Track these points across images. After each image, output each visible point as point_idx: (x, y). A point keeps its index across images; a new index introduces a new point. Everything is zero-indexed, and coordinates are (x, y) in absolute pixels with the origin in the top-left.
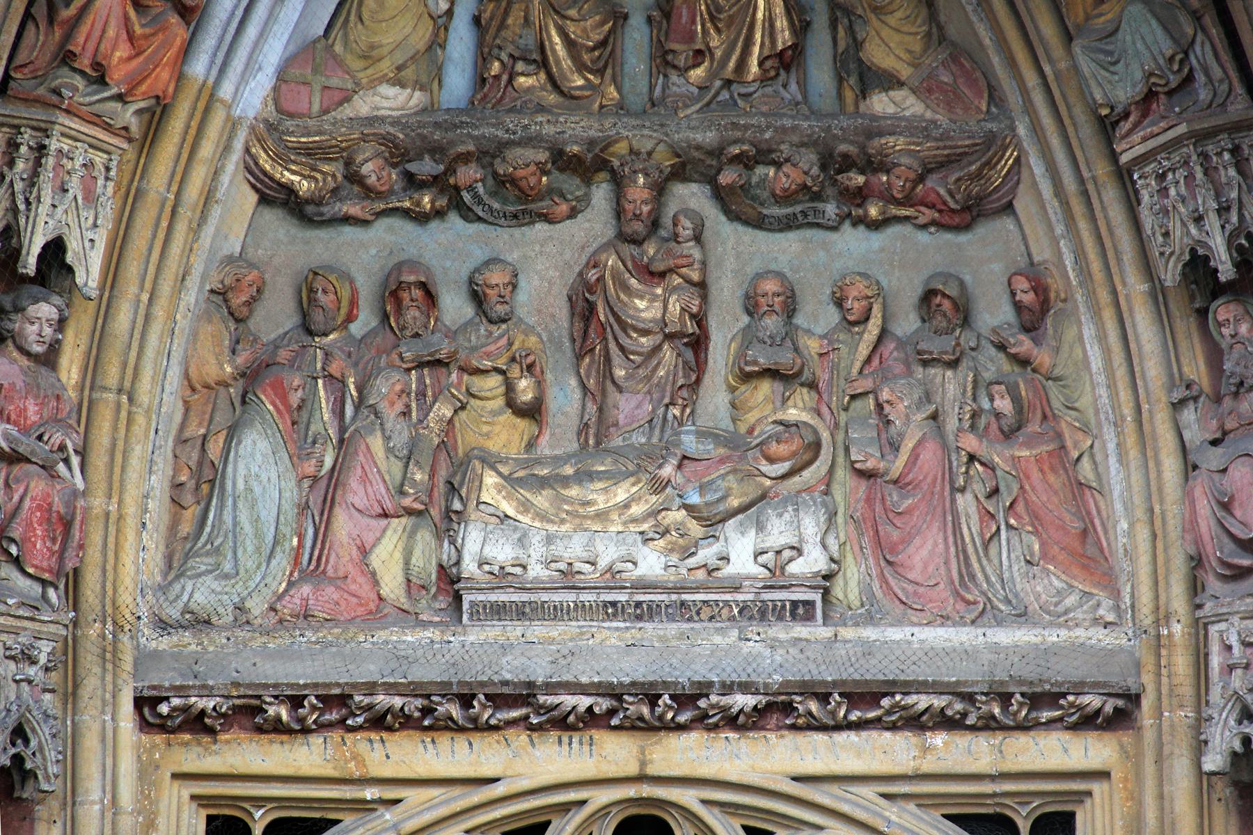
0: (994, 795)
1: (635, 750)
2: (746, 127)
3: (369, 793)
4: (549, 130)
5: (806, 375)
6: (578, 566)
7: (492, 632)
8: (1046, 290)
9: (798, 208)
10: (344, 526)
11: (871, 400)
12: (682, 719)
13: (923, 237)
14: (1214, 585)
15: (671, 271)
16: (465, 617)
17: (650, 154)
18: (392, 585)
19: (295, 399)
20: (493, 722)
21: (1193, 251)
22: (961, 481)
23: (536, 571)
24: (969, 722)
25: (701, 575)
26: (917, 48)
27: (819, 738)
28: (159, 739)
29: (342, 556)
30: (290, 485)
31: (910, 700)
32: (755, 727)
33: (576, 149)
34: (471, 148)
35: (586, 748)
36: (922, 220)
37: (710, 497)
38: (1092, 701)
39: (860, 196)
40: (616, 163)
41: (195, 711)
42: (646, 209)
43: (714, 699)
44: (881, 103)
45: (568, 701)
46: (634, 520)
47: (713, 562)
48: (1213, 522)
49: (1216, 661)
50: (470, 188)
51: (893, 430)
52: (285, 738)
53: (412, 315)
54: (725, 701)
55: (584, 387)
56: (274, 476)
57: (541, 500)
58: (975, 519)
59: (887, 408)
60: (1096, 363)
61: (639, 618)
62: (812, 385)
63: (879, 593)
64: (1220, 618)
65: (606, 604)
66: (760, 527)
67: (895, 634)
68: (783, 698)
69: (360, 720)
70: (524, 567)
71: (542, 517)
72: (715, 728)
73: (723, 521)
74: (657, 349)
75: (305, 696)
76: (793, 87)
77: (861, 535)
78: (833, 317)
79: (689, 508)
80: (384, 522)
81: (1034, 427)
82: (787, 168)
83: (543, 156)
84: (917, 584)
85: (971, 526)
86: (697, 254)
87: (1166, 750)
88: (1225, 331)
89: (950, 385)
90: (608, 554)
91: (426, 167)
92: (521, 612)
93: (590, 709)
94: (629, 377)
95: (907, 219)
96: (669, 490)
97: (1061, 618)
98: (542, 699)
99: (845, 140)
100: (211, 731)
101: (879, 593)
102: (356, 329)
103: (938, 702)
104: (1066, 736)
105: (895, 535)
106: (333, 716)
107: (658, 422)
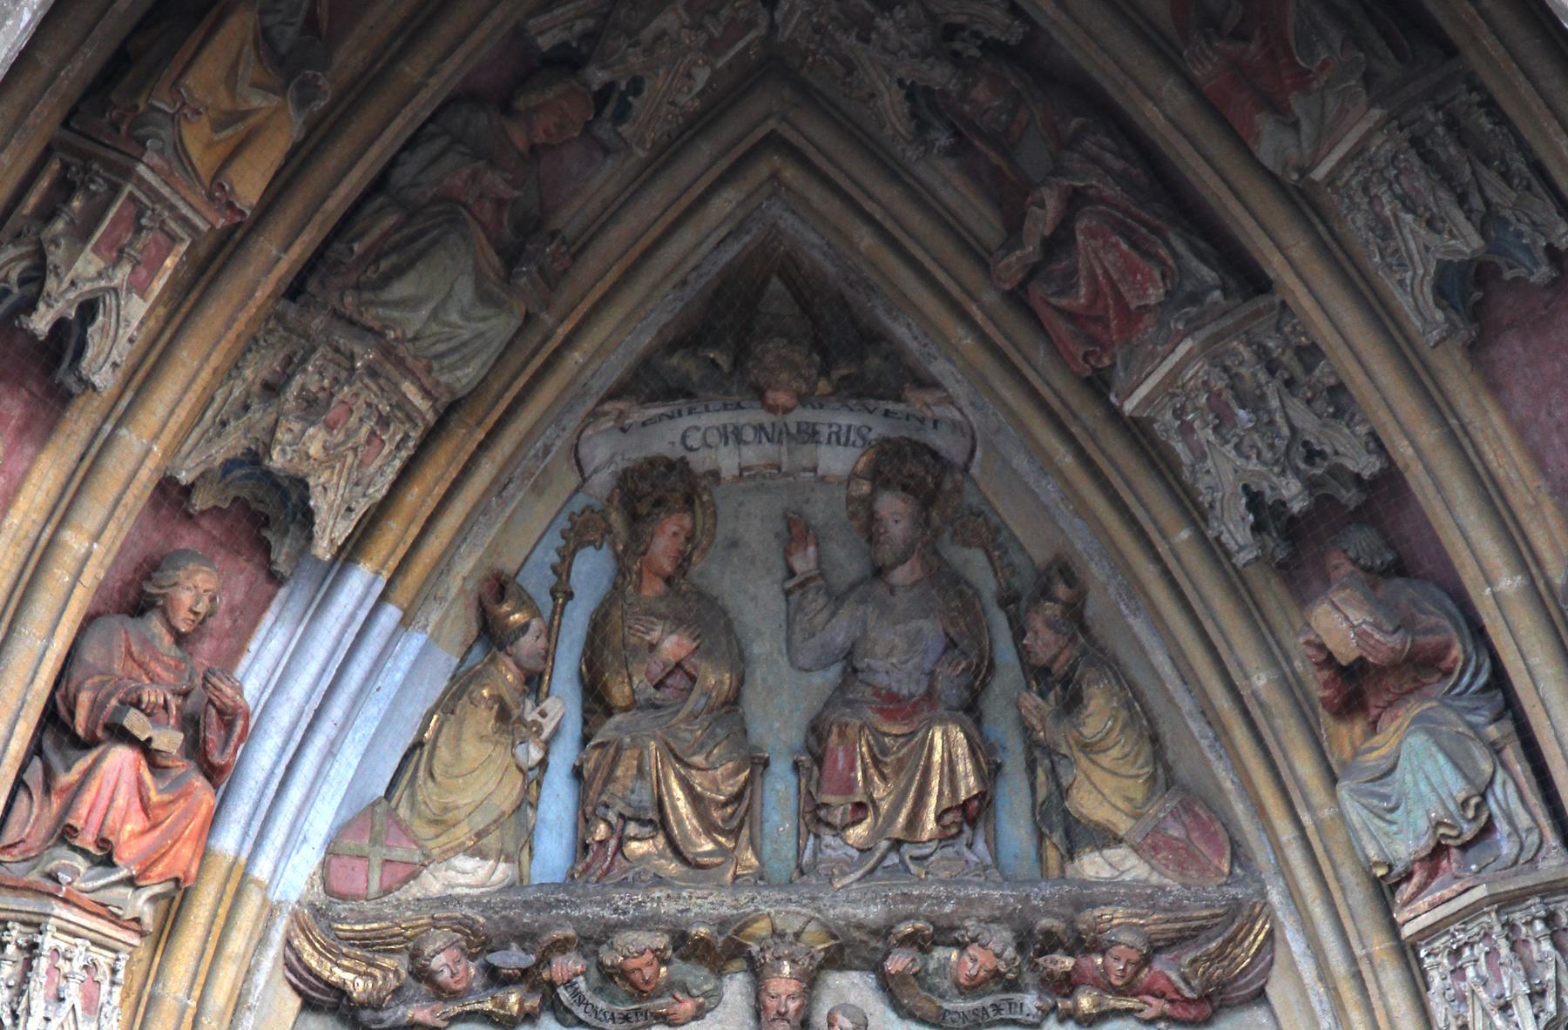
2: (920, 899)
4: (669, 908)
9: (988, 1001)
17: (797, 935)
26: (1138, 794)
33: (703, 930)
34: (571, 932)
36: (1149, 1013)
39: (1067, 984)
40: (755, 948)
42: (793, 1005)
44: (1093, 866)
50: (569, 984)
76: (980, 846)
82: (973, 950)
83: (661, 941)
91: (513, 958)
95: (1128, 1012)
99: (1048, 914)
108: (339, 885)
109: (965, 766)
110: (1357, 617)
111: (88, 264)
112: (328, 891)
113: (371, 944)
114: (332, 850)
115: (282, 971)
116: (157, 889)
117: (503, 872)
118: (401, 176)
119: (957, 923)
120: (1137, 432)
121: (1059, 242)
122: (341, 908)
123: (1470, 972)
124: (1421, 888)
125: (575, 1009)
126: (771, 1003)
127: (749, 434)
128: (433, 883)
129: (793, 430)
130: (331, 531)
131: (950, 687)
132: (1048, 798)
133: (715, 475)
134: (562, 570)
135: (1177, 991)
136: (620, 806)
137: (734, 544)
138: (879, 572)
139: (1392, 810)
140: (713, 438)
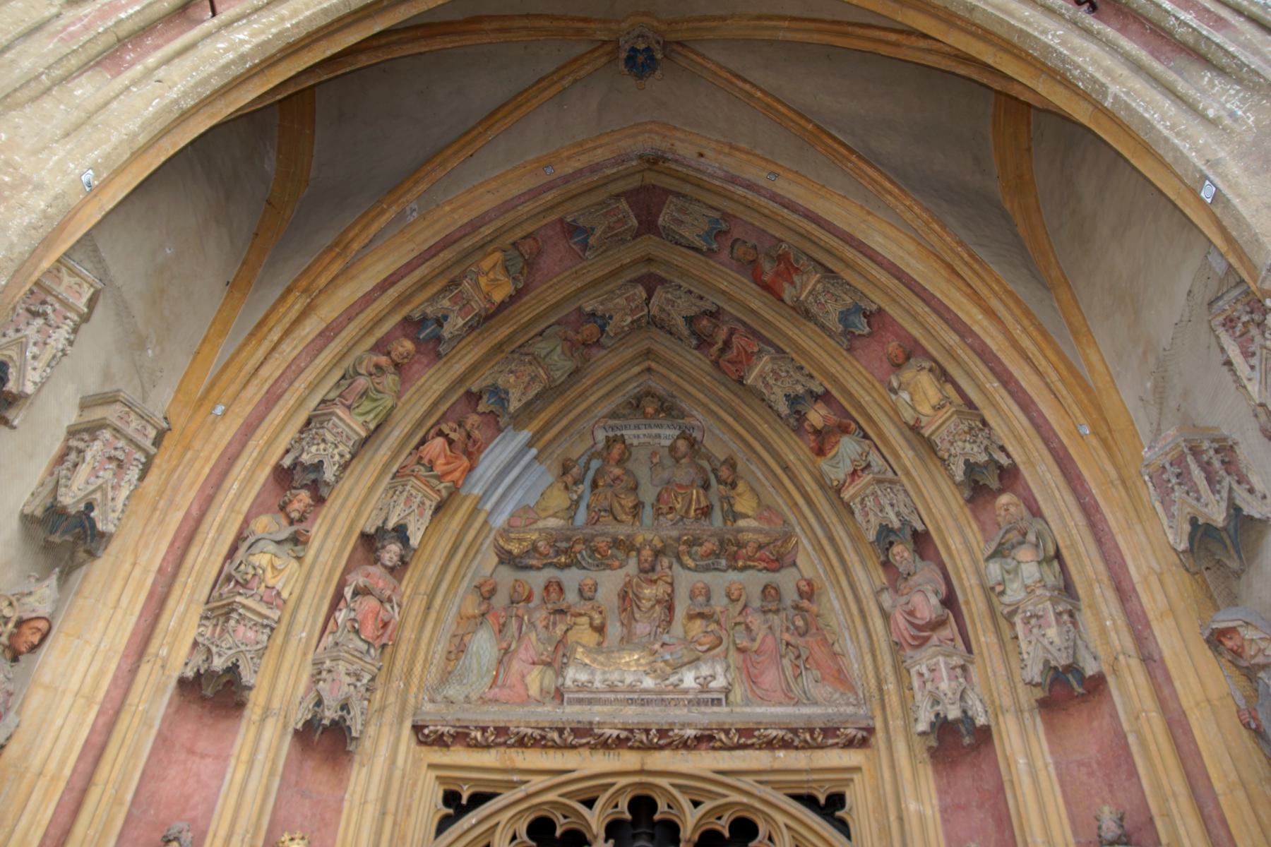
0: (808, 781)
3: (516, 778)
4: (612, 531)
5: (716, 616)
6: (616, 683)
7: (577, 708)
10: (516, 666)
11: (743, 626)
12: (662, 742)
13: (760, 574)
14: (909, 652)
16: (565, 704)
17: (652, 541)
19: (502, 621)
20: (574, 743)
21: (881, 525)
22: (783, 652)
23: (598, 684)
25: (671, 688)
27: (725, 754)
28: (424, 748)
29: (513, 679)
30: (496, 649)
31: (769, 732)
32: (695, 748)
33: (622, 537)
34: (581, 536)
36: (760, 567)
37: (675, 656)
38: (851, 732)
39: (735, 557)
42: (650, 559)
43: (676, 731)
44: (742, 523)
45: (608, 732)
47: (677, 682)
48: (907, 624)
49: (916, 683)
50: (580, 552)
53: (554, 596)
54: (682, 732)
55: (623, 624)
57: (601, 658)
58: (790, 669)
60: (837, 605)
61: (643, 705)
62: (718, 623)
64: (916, 663)
65: (628, 699)
66: (697, 668)
67: (758, 710)
70: (592, 683)
71: (602, 664)
72: (677, 748)
74: (653, 606)
76: (708, 522)
77: (741, 674)
78: (726, 600)
79: (666, 662)
81: (814, 631)
83: (609, 540)
86: (670, 573)
87: (893, 739)
88: (898, 558)
89: (775, 620)
90: (629, 679)
91: (564, 545)
92: (590, 702)
93: (618, 736)
95: (753, 567)
97: (831, 702)
98: (596, 731)
100: (447, 746)
101: (750, 696)
102: (532, 605)
103: (781, 733)
105: (756, 672)
106: (501, 740)
107: (653, 633)
109: (702, 499)
110: (823, 412)
111: (446, 303)
113: (520, 540)
114: (512, 516)
115: (492, 548)
116: (448, 484)
118: (545, 334)
120: (752, 391)
121: (727, 344)
122: (512, 530)
124: (850, 484)
126: (642, 558)
128: (541, 524)
130: (514, 405)
131: (699, 482)
133: (632, 445)
134: (588, 463)
137: (636, 459)
138: (677, 460)
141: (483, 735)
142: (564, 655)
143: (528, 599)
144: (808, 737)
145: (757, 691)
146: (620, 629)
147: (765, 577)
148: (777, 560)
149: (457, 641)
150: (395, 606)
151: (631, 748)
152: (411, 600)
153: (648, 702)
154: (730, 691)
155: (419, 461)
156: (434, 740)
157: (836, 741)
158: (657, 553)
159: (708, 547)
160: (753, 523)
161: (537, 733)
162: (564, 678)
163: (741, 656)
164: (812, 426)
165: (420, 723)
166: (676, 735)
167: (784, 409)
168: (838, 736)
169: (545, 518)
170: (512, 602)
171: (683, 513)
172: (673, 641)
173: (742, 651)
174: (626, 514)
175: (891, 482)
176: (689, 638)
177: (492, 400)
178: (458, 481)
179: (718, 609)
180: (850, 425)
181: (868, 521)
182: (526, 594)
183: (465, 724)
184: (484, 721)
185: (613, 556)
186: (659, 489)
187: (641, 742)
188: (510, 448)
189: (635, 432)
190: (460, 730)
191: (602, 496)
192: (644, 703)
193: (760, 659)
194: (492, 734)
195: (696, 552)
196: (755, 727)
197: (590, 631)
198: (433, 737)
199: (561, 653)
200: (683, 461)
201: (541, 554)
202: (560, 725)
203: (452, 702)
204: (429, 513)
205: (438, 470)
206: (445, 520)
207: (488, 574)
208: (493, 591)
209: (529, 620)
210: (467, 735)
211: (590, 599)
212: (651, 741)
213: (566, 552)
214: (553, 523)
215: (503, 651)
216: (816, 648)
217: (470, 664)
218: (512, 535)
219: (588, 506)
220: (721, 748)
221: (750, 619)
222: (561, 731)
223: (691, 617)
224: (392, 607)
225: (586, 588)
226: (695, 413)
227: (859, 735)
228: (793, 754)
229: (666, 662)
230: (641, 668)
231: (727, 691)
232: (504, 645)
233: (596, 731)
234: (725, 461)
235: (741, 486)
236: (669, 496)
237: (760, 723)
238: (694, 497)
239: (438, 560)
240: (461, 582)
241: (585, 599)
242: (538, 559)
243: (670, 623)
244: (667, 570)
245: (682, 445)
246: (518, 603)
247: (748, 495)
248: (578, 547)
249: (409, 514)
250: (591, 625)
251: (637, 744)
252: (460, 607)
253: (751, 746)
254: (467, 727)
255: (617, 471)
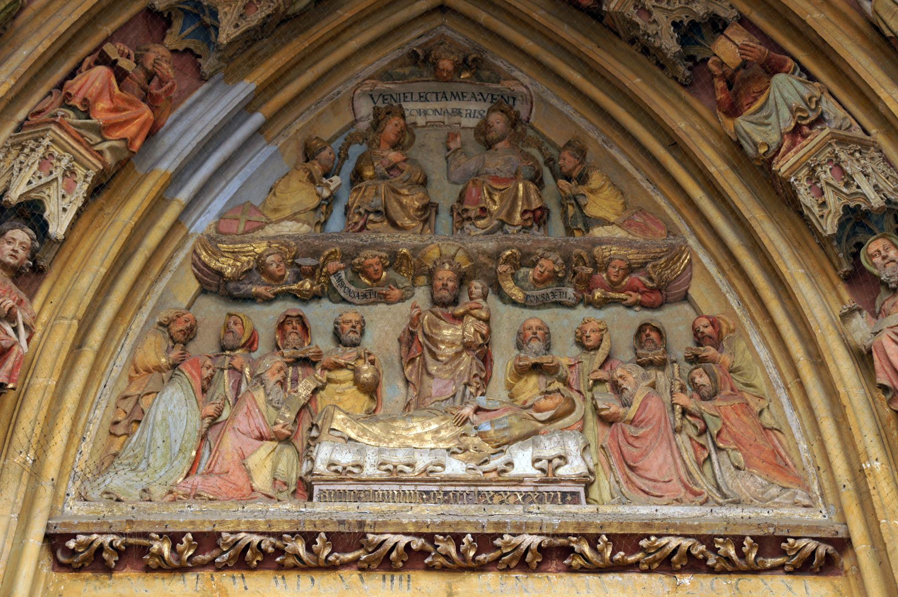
1: (444, 585)
2: (514, 240)
4: (387, 240)
5: (561, 372)
8: (719, 325)
9: (550, 290)
10: (230, 443)
11: (608, 386)
13: (631, 313)
15: (467, 313)
16: (315, 499)
17: (453, 257)
18: (262, 481)
19: (206, 373)
20: (331, 558)
21: (846, 208)
23: (370, 471)
24: (710, 563)
25: (493, 475)
27: (591, 579)
28: (66, 576)
31: (664, 541)
32: (539, 568)
33: (405, 251)
35: (405, 583)
36: (630, 300)
37: (496, 427)
39: (587, 285)
41: (95, 545)
42: (450, 284)
44: (598, 232)
46: (442, 440)
47: (502, 467)
50: (336, 273)
51: (626, 394)
52: (166, 575)
53: (293, 338)
54: (516, 540)
55: (407, 382)
56: (184, 412)
57: (376, 430)
58: (691, 451)
59: (620, 381)
61: (447, 502)
62: (565, 382)
63: (625, 489)
65: (421, 493)
68: (561, 541)
69: (226, 556)
70: (360, 467)
71: (376, 438)
72: (508, 569)
73: (509, 443)
74: (458, 354)
75: (184, 534)
78: (576, 350)
79: (482, 435)
80: (258, 443)
83: (384, 254)
84: (655, 481)
85: (689, 456)
86: (484, 304)
88: (877, 260)
89: (661, 378)
90: (423, 461)
91: (307, 262)
92: (357, 497)
93: (408, 546)
94: (438, 370)
96: (468, 425)
97: (765, 502)
99: (577, 246)
100: (108, 570)
101: (625, 489)
103: (686, 543)
104: (788, 579)
108: (221, 229)
109: (533, 197)
110: (739, 40)
112: (218, 231)
114: (222, 216)
115: (189, 266)
117: (305, 228)
119: (533, 251)
122: (224, 238)
123: (823, 176)
124: (789, 149)
125: (339, 289)
127: (430, 112)
128: (270, 231)
129: (450, 111)
130: (227, 33)
131: (526, 171)
132: (574, 216)
133: (415, 124)
134: (345, 149)
135: (645, 286)
136: (366, 207)
139: (767, 117)
140: (414, 113)
141: (173, 549)
142: (313, 426)
143: (250, 345)
144: (732, 552)
145: (639, 482)
146: (403, 391)
147: (639, 316)
148: (659, 289)
149: (128, 405)
150: (22, 329)
151: (430, 568)
152: (50, 327)
153: (457, 497)
154: (591, 483)
155: (65, 103)
156: (85, 560)
157: (780, 560)
158: (463, 279)
159: (546, 265)
160: (619, 233)
161: (268, 544)
162: (313, 461)
163: (607, 431)
164: (722, 64)
165: (59, 530)
166: (507, 544)
167: (670, 44)
168: (783, 553)
169: (278, 222)
170: (223, 349)
171: (503, 216)
172: (497, 405)
173: (607, 421)
174: (410, 217)
175: (859, 142)
176: (519, 404)
177: (189, 30)
178: (133, 139)
179: (564, 361)
180: (786, 61)
181: (824, 204)
182: (247, 336)
183: (141, 529)
184: (174, 524)
185: (388, 281)
186: (461, 187)
187: (447, 557)
188: (219, 107)
189: (420, 106)
190: (131, 541)
191: (370, 193)
192: (448, 498)
193: (641, 432)
194: (190, 546)
195: (526, 276)
196: (641, 532)
197: (355, 388)
198: (84, 554)
199: (307, 425)
200: (500, 145)
201: (271, 276)
202: (309, 528)
203: (118, 500)
204: (82, 189)
205: (100, 117)
206: (109, 210)
207: (185, 304)
208: (190, 334)
209: (252, 375)
210: (145, 549)
211: (355, 345)
212: (462, 554)
213: (311, 274)
214: (289, 228)
215: (207, 420)
216: (733, 416)
217: (152, 438)
218: (223, 247)
219: (347, 208)
220: (583, 570)
221: (619, 372)
222: (309, 538)
223: (522, 371)
224: (16, 330)
225: (348, 327)
226: (517, 74)
227: (822, 550)
228: (706, 581)
229: (482, 435)
230: (441, 445)
231: (588, 482)
232: (210, 410)
233: (370, 537)
234: (569, 144)
235: (596, 180)
236: (479, 193)
237: (649, 525)
238: (521, 193)
239: (98, 267)
240: (136, 314)
241: (345, 346)
242: (264, 284)
243: (486, 381)
244: (480, 300)
245: (498, 121)
246: (233, 349)
247: (607, 192)
248: (332, 266)
249: (48, 184)
250: (356, 381)
251: (441, 560)
252: (134, 349)
253: (634, 567)
254: (146, 535)
255: (394, 156)
